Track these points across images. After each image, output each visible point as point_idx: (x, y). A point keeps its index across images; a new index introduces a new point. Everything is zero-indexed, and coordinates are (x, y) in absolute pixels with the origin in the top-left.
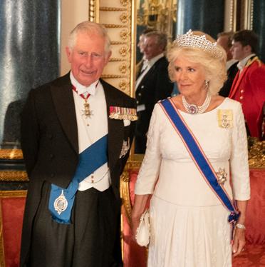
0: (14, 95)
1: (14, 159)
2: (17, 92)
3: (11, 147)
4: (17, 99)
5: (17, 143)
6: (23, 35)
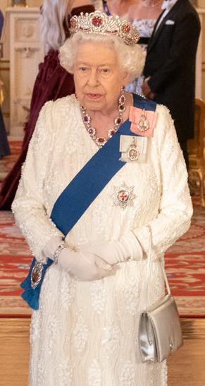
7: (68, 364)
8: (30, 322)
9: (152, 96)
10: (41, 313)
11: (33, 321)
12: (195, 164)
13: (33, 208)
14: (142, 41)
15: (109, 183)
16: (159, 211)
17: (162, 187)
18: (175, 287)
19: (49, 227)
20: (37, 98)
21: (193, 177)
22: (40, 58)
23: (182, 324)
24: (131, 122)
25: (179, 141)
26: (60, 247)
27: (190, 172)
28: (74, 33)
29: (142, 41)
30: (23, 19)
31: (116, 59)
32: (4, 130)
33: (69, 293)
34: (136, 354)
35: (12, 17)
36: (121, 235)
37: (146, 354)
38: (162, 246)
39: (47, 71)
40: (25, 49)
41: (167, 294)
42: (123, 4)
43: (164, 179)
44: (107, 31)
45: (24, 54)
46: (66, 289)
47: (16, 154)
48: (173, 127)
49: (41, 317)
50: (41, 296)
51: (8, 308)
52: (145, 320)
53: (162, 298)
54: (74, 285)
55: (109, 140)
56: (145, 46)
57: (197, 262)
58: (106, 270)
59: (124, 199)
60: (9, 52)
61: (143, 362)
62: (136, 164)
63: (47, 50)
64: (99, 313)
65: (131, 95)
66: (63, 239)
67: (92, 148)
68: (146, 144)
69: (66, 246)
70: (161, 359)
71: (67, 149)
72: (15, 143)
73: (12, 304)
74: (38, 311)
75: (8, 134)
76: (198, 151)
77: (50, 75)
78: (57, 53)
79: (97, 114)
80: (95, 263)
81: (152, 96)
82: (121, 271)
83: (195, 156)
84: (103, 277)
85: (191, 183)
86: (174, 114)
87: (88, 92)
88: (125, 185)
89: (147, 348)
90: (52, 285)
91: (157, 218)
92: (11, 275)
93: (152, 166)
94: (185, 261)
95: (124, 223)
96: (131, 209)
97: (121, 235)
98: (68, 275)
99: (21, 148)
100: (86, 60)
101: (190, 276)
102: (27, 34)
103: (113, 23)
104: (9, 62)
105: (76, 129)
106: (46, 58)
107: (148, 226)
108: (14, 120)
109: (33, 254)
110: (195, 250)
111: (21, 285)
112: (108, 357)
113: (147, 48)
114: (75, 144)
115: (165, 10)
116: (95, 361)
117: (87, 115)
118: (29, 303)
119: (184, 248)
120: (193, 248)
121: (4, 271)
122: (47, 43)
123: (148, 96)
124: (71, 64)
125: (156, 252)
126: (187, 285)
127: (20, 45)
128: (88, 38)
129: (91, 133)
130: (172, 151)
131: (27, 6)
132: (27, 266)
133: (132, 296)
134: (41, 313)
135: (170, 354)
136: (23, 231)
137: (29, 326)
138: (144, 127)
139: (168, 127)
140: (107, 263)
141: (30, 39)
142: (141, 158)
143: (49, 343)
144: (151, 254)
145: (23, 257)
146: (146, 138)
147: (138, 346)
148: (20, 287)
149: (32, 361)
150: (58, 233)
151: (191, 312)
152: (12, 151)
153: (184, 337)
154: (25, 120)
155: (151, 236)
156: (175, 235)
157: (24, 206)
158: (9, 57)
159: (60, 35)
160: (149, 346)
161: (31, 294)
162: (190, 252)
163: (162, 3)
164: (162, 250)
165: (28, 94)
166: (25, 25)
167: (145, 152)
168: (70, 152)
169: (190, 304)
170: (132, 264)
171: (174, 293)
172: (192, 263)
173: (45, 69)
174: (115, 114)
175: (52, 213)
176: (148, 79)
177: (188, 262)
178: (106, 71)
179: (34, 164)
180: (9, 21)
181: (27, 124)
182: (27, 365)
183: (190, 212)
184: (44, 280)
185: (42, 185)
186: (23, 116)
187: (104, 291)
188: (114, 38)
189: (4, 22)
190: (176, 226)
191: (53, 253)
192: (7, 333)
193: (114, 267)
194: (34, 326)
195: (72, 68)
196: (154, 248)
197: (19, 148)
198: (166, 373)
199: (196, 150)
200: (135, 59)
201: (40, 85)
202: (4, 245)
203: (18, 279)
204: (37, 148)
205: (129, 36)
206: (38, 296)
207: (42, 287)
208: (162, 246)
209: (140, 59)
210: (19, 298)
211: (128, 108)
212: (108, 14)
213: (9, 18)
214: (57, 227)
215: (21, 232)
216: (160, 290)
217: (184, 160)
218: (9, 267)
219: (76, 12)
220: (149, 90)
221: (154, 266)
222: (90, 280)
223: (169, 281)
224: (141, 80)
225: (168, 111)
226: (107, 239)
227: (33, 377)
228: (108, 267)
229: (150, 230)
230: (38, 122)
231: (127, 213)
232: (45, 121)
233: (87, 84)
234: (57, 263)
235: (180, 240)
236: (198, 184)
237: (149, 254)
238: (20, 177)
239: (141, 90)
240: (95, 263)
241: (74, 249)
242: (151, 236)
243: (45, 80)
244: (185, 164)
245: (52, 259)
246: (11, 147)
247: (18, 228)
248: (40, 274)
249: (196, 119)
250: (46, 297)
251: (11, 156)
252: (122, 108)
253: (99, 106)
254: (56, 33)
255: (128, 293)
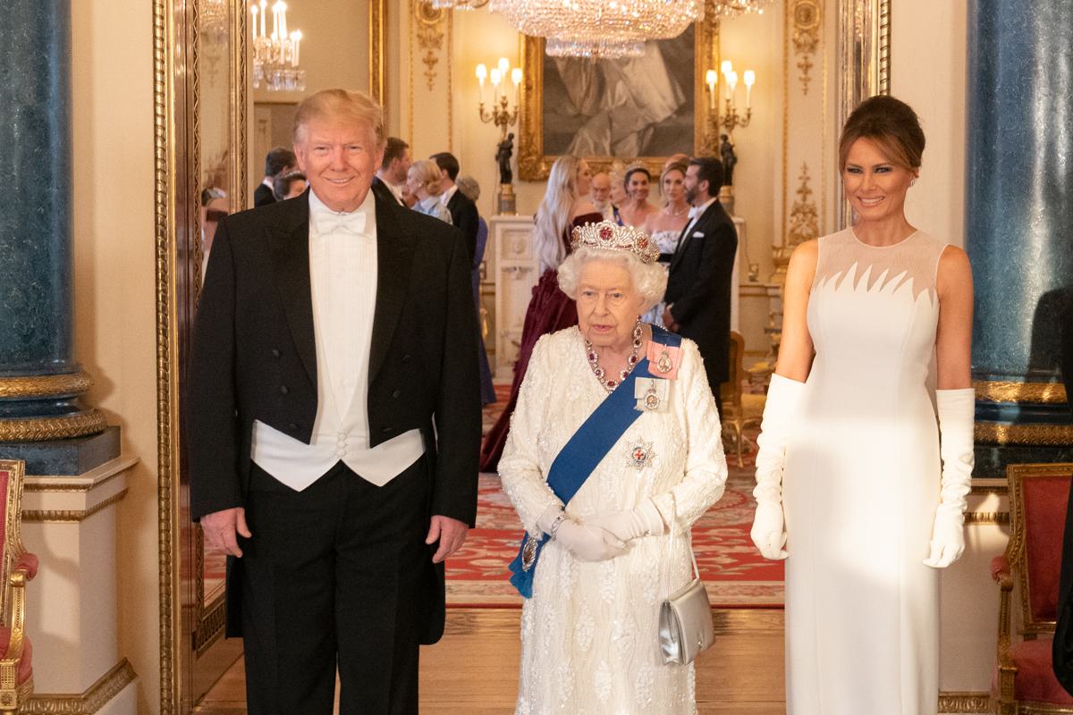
0: (1049, 279)
1: (1050, 401)
2: (1055, 272)
3: (1045, 379)
4: (1055, 286)
5: (1057, 372)
6: (1067, 162)
7: (569, 667)
8: (521, 613)
9: (676, 327)
10: (535, 602)
11: (524, 612)
12: (730, 413)
13: (525, 469)
14: (664, 258)
15: (622, 437)
16: (685, 473)
17: (688, 442)
18: (704, 570)
19: (544, 494)
20: (530, 332)
21: (727, 431)
22: (533, 279)
23: (715, 616)
24: (648, 362)
25: (710, 385)
26: (559, 518)
27: (724, 424)
28: (577, 247)
29: (664, 258)
30: (512, 231)
31: (630, 281)
32: (489, 371)
33: (570, 576)
34: (656, 654)
35: (499, 228)
36: (637, 502)
37: (668, 654)
38: (689, 517)
39: (542, 296)
40: (515, 269)
41: (694, 578)
42: (639, 212)
43: (691, 433)
44: (618, 246)
45: (514, 275)
46: (567, 571)
47: (504, 401)
48: (702, 367)
49: (535, 608)
50: (535, 580)
51: (493, 596)
52: (667, 610)
53: (689, 583)
54: (577, 568)
55: (622, 384)
56: (668, 264)
57: (733, 538)
58: (617, 548)
59: (640, 458)
60: (494, 272)
61: (665, 665)
62: (655, 414)
63: (543, 270)
64: (610, 602)
65: (650, 327)
66: (563, 509)
67: (600, 394)
68: (668, 388)
69: (567, 518)
70: (687, 660)
71: (568, 394)
72: (502, 387)
73: (498, 591)
74: (532, 600)
75: (493, 375)
76: (734, 397)
77: (546, 302)
78: (556, 273)
79: (605, 350)
80: (604, 540)
81: (676, 327)
82: (637, 548)
83: (730, 403)
84: (613, 557)
85: (726, 438)
86: (703, 351)
87: (595, 322)
88: (641, 441)
89: (669, 646)
90: (549, 567)
91: (682, 482)
92: (496, 554)
93: (676, 417)
94: (717, 536)
95: (640, 489)
96: (649, 470)
97: (637, 502)
98: (569, 555)
99: (509, 393)
100: (591, 283)
101: (724, 556)
102: (517, 250)
103: (626, 236)
104: (494, 284)
105: (580, 369)
106: (541, 280)
107: (671, 493)
108: (501, 358)
109: (525, 528)
110: (730, 523)
111: (510, 567)
112: (620, 658)
113: (670, 268)
114: (578, 388)
115: (692, 219)
116: (603, 663)
117: (593, 352)
118: (519, 590)
119: (716, 521)
120: (728, 520)
121: (489, 550)
122: (544, 261)
123: (670, 328)
124: (573, 288)
125: (681, 525)
126: (720, 567)
127: (509, 264)
128: (595, 254)
129: (598, 374)
130: (702, 398)
131: (517, 215)
132: (517, 543)
133: (650, 581)
134: (535, 602)
135: (699, 654)
136: (512, 498)
137: (519, 618)
138: (667, 367)
139: (696, 367)
140: (618, 539)
141: (521, 256)
142: (663, 406)
143: (546, 640)
144: (674, 528)
145: (513, 531)
146: (668, 381)
147: (657, 644)
148: (508, 569)
149: (524, 663)
150: (557, 502)
151: (726, 601)
152: (498, 398)
153: (716, 632)
154: (514, 359)
155: (675, 505)
156: (705, 504)
157: (514, 468)
158: (495, 278)
159: (560, 251)
160: (672, 645)
161: (523, 578)
162: (723, 525)
163: (688, 211)
164: (689, 523)
165: (519, 326)
166: (515, 238)
167: (666, 399)
168: (571, 399)
169: (725, 591)
170: (650, 540)
171: (703, 577)
172: (726, 539)
173: (540, 293)
174: (629, 351)
175: (549, 476)
176: (670, 306)
177: (721, 537)
178: (617, 296)
179: (526, 413)
180: (494, 232)
181: (517, 363)
182: (517, 668)
183: (725, 474)
184: (539, 561)
185: (536, 440)
186: (512, 353)
187: (615, 574)
188: (628, 254)
189: (489, 234)
190: (706, 492)
191: (550, 527)
192: (492, 627)
193: (628, 544)
194: (526, 619)
195: (575, 293)
196: (678, 519)
197: (507, 393)
198: (694, 678)
199: (732, 396)
200: (654, 281)
201: (534, 313)
202: (488, 517)
203: (506, 560)
204: (530, 394)
205: (647, 251)
206: (531, 582)
207: (537, 569)
208: (689, 517)
209: (661, 281)
210: (507, 583)
211: (645, 342)
212: (620, 224)
213: (494, 228)
214: (555, 493)
215: (509, 500)
216: (686, 573)
217: (717, 409)
218: (494, 544)
219: (580, 221)
220: (672, 320)
221: (678, 542)
222: (597, 561)
223: (697, 562)
224: (662, 308)
225: (697, 347)
226: (619, 508)
227: (525, 683)
228: (620, 544)
229: (674, 498)
230: (531, 360)
231: (644, 476)
232: (540, 360)
233: (593, 313)
234: (555, 539)
235: (711, 509)
236: (734, 439)
237: (671, 528)
238: (508, 431)
239: (661, 320)
240: (604, 540)
241: (577, 522)
242: (675, 505)
243: (540, 307)
244: (718, 414)
245: (549, 533)
246: (497, 392)
247: (506, 495)
248: (534, 553)
249: (732, 357)
250: (542, 582)
251: (496, 404)
252: (637, 343)
253: (608, 340)
254: (553, 248)
255: (645, 576)
